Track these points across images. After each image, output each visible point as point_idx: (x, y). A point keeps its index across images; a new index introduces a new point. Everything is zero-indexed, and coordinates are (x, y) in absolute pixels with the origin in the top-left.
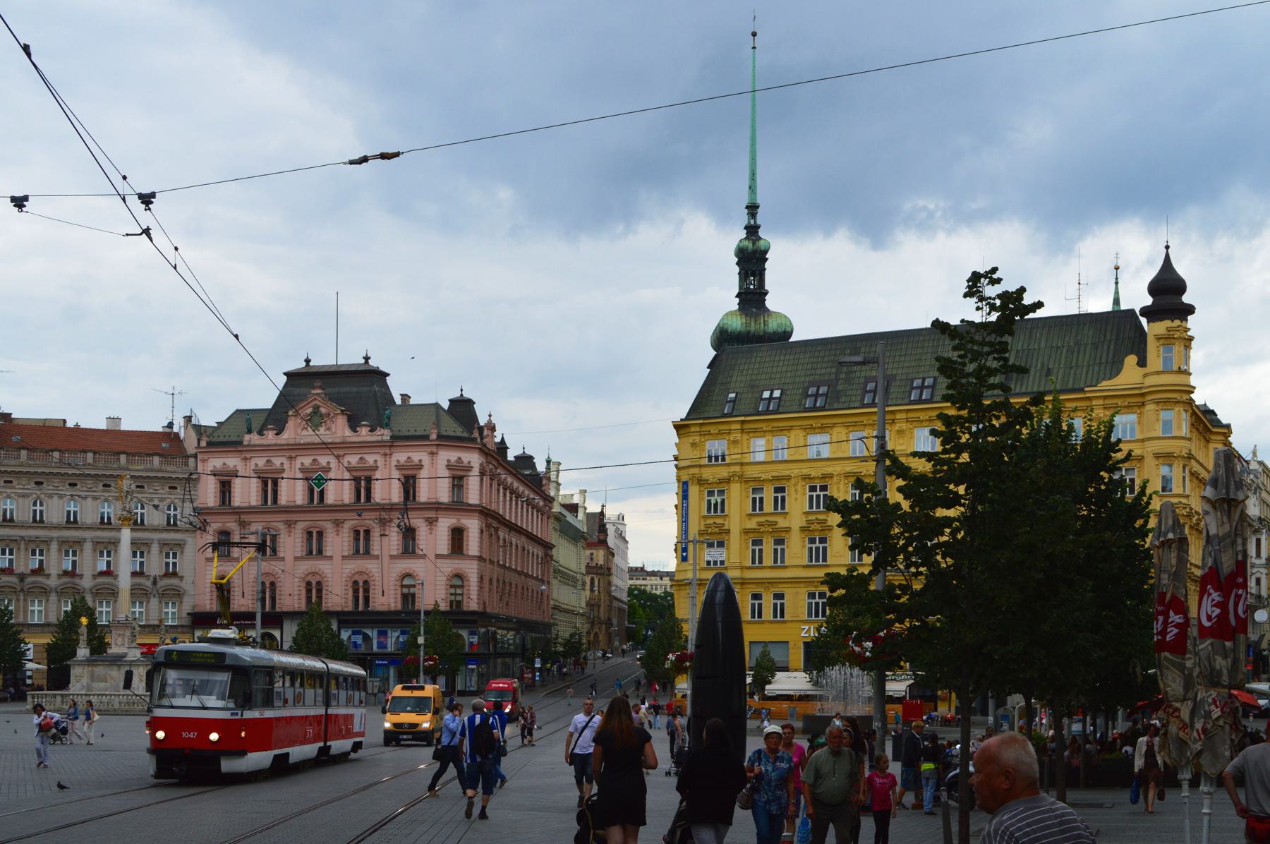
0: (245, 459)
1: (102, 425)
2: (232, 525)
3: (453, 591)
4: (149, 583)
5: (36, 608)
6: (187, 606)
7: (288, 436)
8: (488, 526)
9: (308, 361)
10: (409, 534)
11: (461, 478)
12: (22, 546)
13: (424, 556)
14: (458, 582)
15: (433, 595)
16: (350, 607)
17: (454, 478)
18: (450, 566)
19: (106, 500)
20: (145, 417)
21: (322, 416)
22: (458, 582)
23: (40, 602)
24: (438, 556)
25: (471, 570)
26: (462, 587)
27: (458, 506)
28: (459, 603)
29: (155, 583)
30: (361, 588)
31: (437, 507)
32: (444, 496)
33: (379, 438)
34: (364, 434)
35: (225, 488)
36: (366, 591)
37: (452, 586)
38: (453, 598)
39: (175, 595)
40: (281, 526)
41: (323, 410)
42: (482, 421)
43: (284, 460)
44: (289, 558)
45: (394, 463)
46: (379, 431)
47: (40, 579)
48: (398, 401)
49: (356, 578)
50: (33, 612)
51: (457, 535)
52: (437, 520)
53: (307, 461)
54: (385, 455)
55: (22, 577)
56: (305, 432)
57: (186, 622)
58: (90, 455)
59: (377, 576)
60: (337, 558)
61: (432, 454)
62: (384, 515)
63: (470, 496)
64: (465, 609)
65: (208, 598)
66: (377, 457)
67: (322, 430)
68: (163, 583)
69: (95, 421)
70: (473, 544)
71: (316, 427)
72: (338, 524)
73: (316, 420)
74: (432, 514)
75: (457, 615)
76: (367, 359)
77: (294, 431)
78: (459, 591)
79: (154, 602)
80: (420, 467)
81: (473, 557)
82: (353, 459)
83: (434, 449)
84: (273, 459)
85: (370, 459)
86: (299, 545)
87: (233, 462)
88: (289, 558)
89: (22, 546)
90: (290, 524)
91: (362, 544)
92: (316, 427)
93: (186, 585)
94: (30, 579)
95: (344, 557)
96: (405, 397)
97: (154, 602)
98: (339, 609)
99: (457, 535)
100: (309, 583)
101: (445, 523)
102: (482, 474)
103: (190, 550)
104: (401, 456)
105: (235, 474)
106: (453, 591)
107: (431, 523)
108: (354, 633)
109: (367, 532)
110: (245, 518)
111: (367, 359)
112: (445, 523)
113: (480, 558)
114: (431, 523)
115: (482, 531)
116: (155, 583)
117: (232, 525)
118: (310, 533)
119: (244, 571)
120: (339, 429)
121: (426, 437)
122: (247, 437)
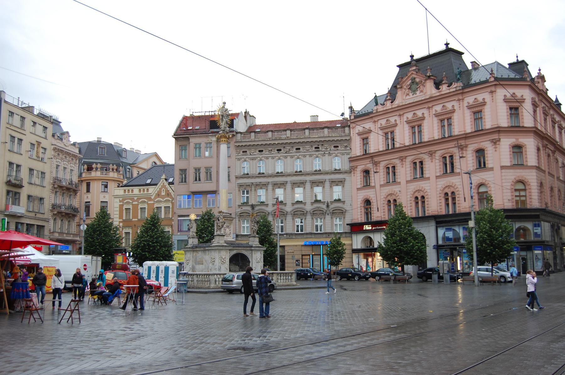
0: (375, 122)
1: (309, 120)
2: (370, 166)
3: (517, 194)
4: (324, 207)
5: (246, 225)
6: (348, 220)
7: (397, 102)
8: (545, 147)
9: (412, 56)
10: (480, 152)
11: (517, 109)
12: (253, 188)
13: (492, 169)
14: (521, 186)
15: (503, 199)
16: (443, 212)
17: (511, 109)
18: (512, 175)
19: (298, 158)
20: (332, 112)
21: (417, 84)
22: (521, 186)
23: (248, 221)
24: (503, 167)
25: (532, 177)
26: (525, 190)
27: (516, 129)
28: (524, 202)
29: (328, 206)
30: (450, 197)
31: (498, 130)
32: (504, 121)
33: (454, 90)
34: (444, 89)
35: (365, 141)
36: (454, 199)
37: (516, 190)
38: (518, 198)
39: (341, 213)
40: (397, 162)
41: (417, 80)
42: (534, 74)
43: (397, 118)
44: (403, 182)
45: (466, 104)
46: (454, 85)
47: (263, 207)
48: (470, 67)
49: (446, 190)
50: (244, 227)
51: (518, 149)
52: (499, 140)
53: (410, 116)
54: (459, 100)
55: (253, 207)
56: (408, 97)
57: (348, 229)
58: (288, 132)
59: (460, 188)
60: (433, 178)
61: (492, 92)
62: (462, 142)
63: (525, 121)
64: (528, 207)
65: (359, 214)
66: (454, 103)
67: (418, 93)
68: (332, 206)
69: (304, 118)
70: (531, 157)
71: (414, 92)
72: (431, 154)
73: (414, 87)
74: (495, 136)
75: (520, 213)
76: (447, 44)
77: (401, 99)
78: (523, 193)
79: (328, 217)
80: (484, 104)
81: (532, 167)
82: (438, 108)
83: (493, 89)
84: (390, 119)
85: (449, 106)
86: (408, 172)
87: (368, 125)
88: (403, 182)
89: (253, 188)
90: (402, 159)
91: (449, 166)
92: (414, 92)
93: (346, 207)
94: (257, 208)
95: (437, 177)
96: (473, 63)
97: (328, 217)
98: (436, 213)
99: (518, 149)
100: (417, 198)
101: (506, 142)
102: (535, 105)
103: (347, 184)
104: (470, 99)
105: (370, 131)
106: (517, 194)
107: (495, 143)
108: (448, 230)
109: (451, 157)
110: (376, 159)
111: (447, 44)
112: (506, 142)
113: (538, 168)
114: (495, 143)
115: (538, 149)
116: (328, 206)
117: (370, 166)
118: (415, 163)
119: (379, 195)
120: (430, 89)
121: (486, 81)
122: (375, 108)
